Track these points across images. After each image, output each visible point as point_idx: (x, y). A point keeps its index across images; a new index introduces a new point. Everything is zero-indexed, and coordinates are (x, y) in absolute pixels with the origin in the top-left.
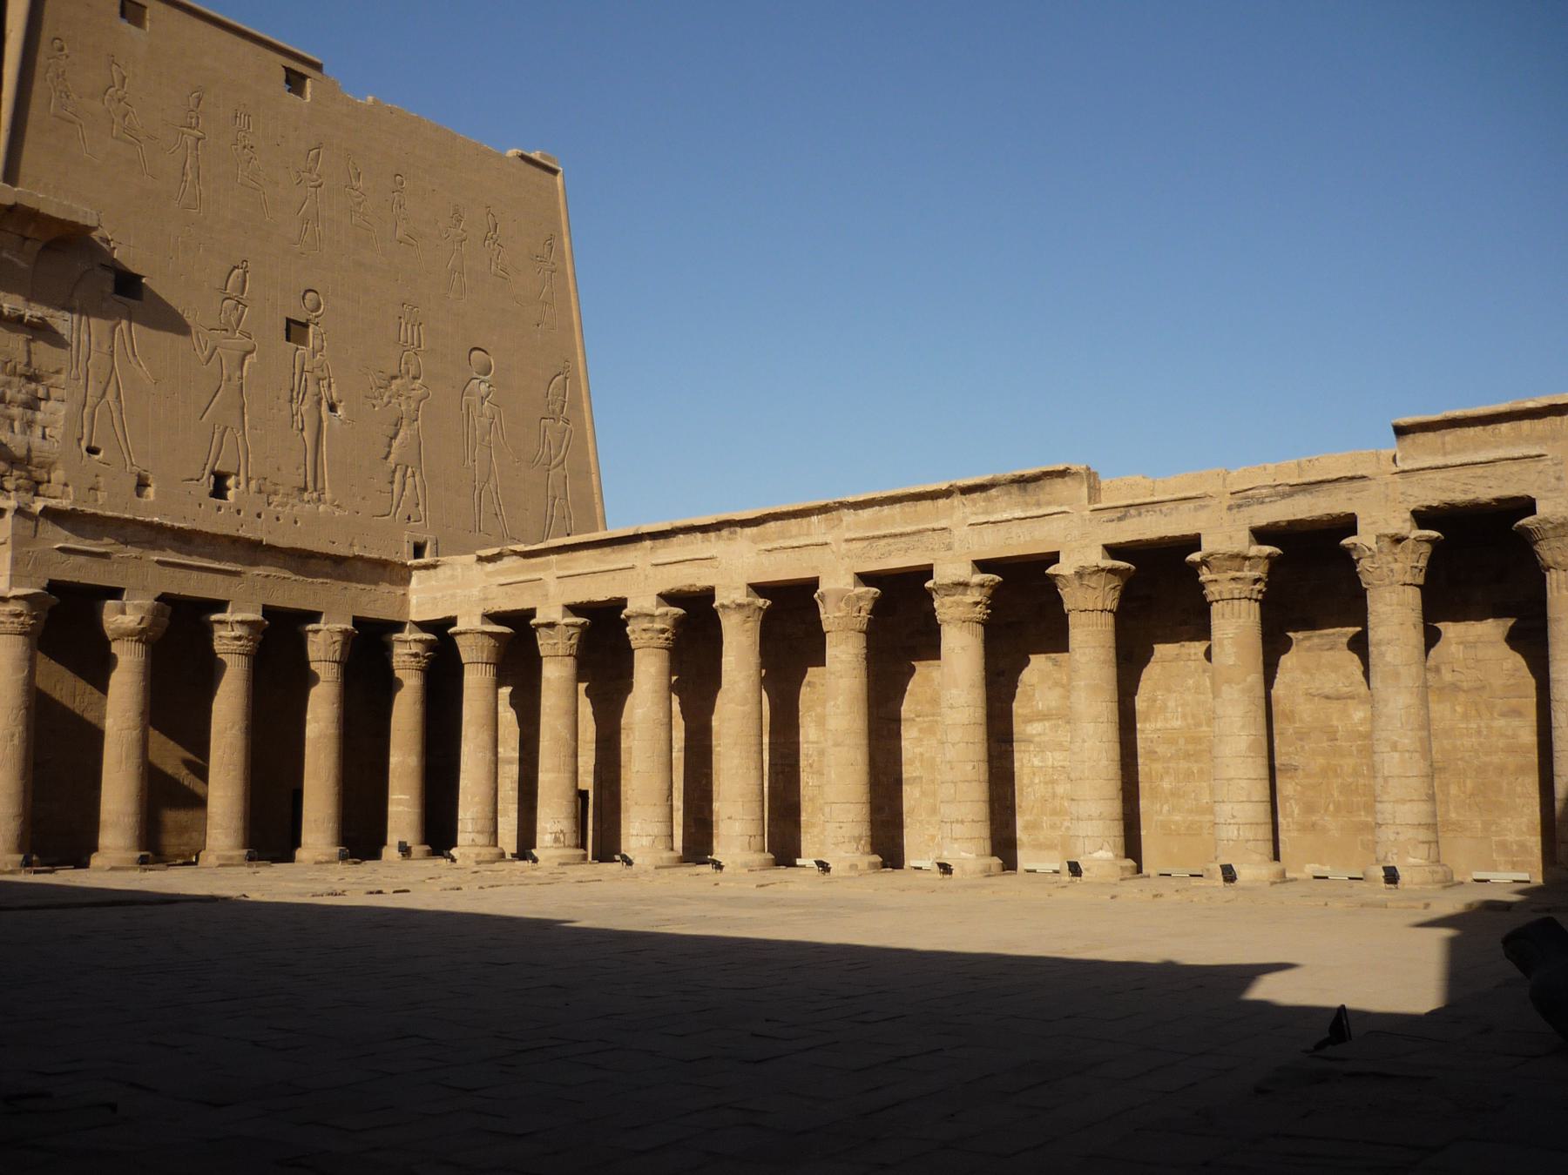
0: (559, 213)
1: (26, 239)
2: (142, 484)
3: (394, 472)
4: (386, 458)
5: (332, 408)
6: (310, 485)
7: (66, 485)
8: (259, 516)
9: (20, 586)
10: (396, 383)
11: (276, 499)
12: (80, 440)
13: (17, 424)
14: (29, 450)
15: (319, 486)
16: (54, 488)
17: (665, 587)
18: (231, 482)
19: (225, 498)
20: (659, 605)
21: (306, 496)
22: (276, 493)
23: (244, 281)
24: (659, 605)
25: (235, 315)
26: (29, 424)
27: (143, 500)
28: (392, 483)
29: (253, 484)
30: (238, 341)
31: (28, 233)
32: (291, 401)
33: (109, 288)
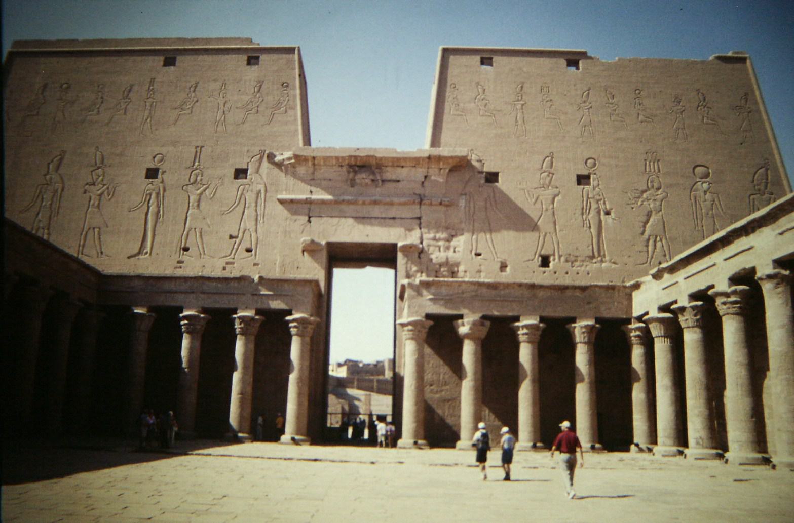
0: (750, 80)
1: (441, 169)
2: (503, 267)
3: (648, 240)
4: (643, 233)
5: (608, 213)
6: (596, 254)
7: (465, 272)
8: (567, 273)
9: (412, 316)
10: (645, 196)
11: (577, 264)
12: (471, 251)
13: (442, 249)
14: (447, 259)
15: (602, 254)
16: (461, 274)
17: (731, 273)
18: (551, 259)
19: (548, 267)
20: (730, 286)
21: (594, 261)
22: (576, 261)
23: (552, 163)
24: (730, 286)
25: (549, 179)
26: (448, 248)
27: (503, 274)
28: (647, 246)
29: (563, 259)
30: (551, 191)
31: (441, 167)
32: (583, 214)
33: (483, 181)
